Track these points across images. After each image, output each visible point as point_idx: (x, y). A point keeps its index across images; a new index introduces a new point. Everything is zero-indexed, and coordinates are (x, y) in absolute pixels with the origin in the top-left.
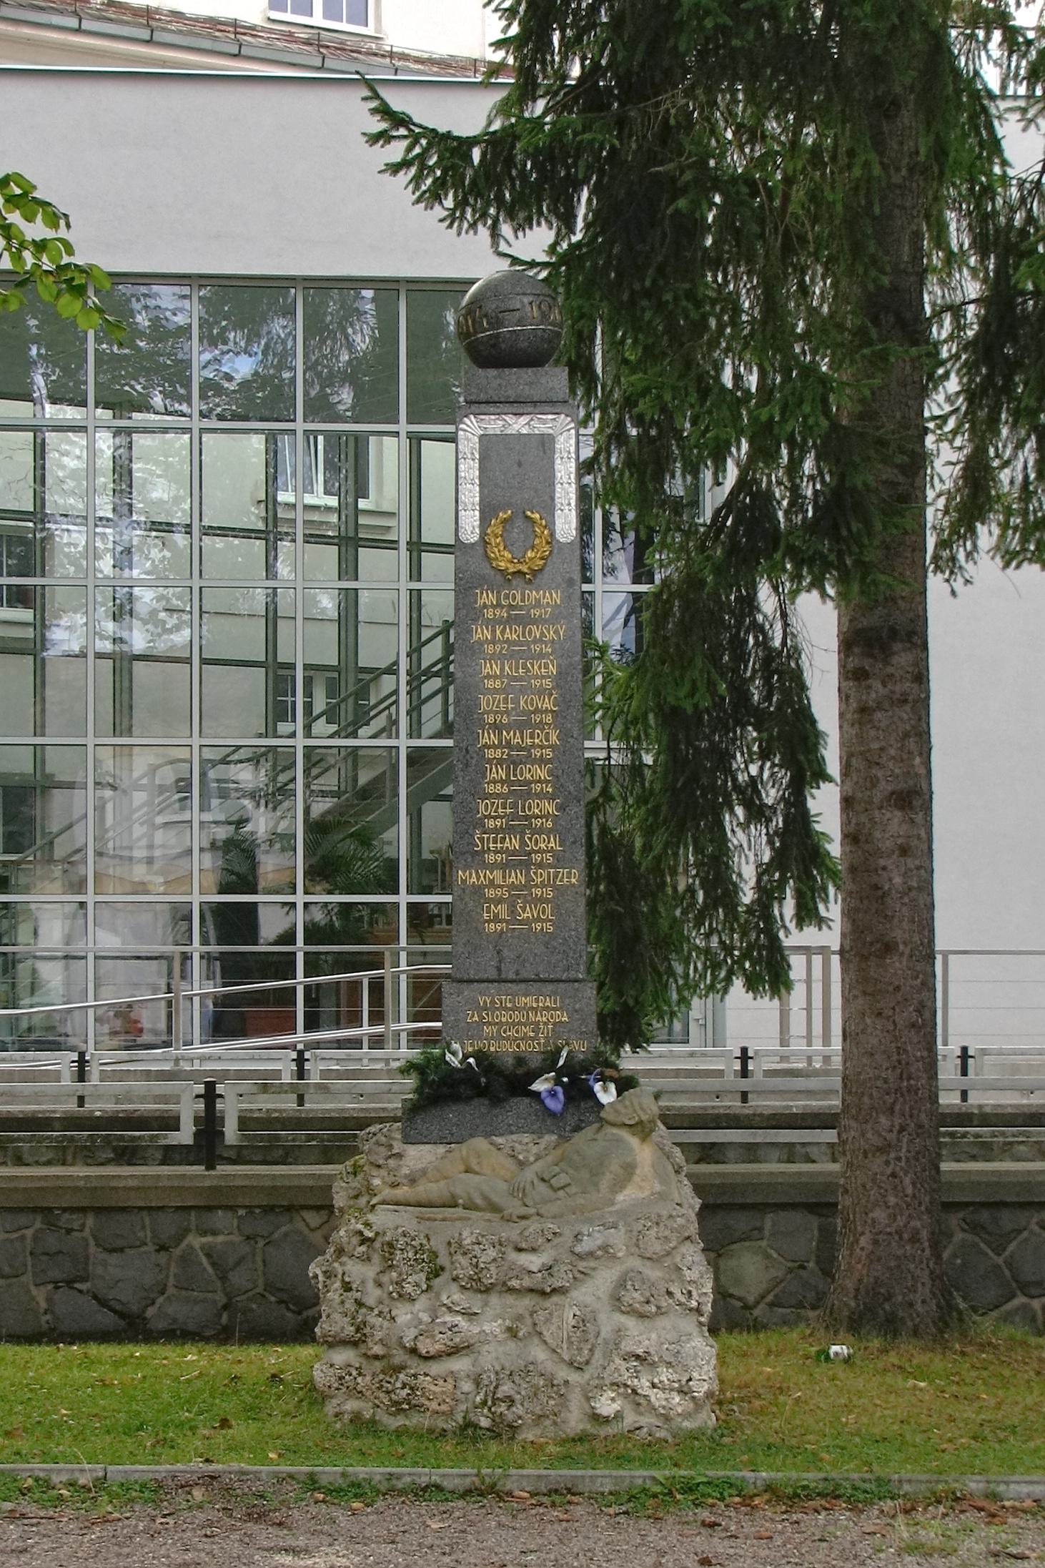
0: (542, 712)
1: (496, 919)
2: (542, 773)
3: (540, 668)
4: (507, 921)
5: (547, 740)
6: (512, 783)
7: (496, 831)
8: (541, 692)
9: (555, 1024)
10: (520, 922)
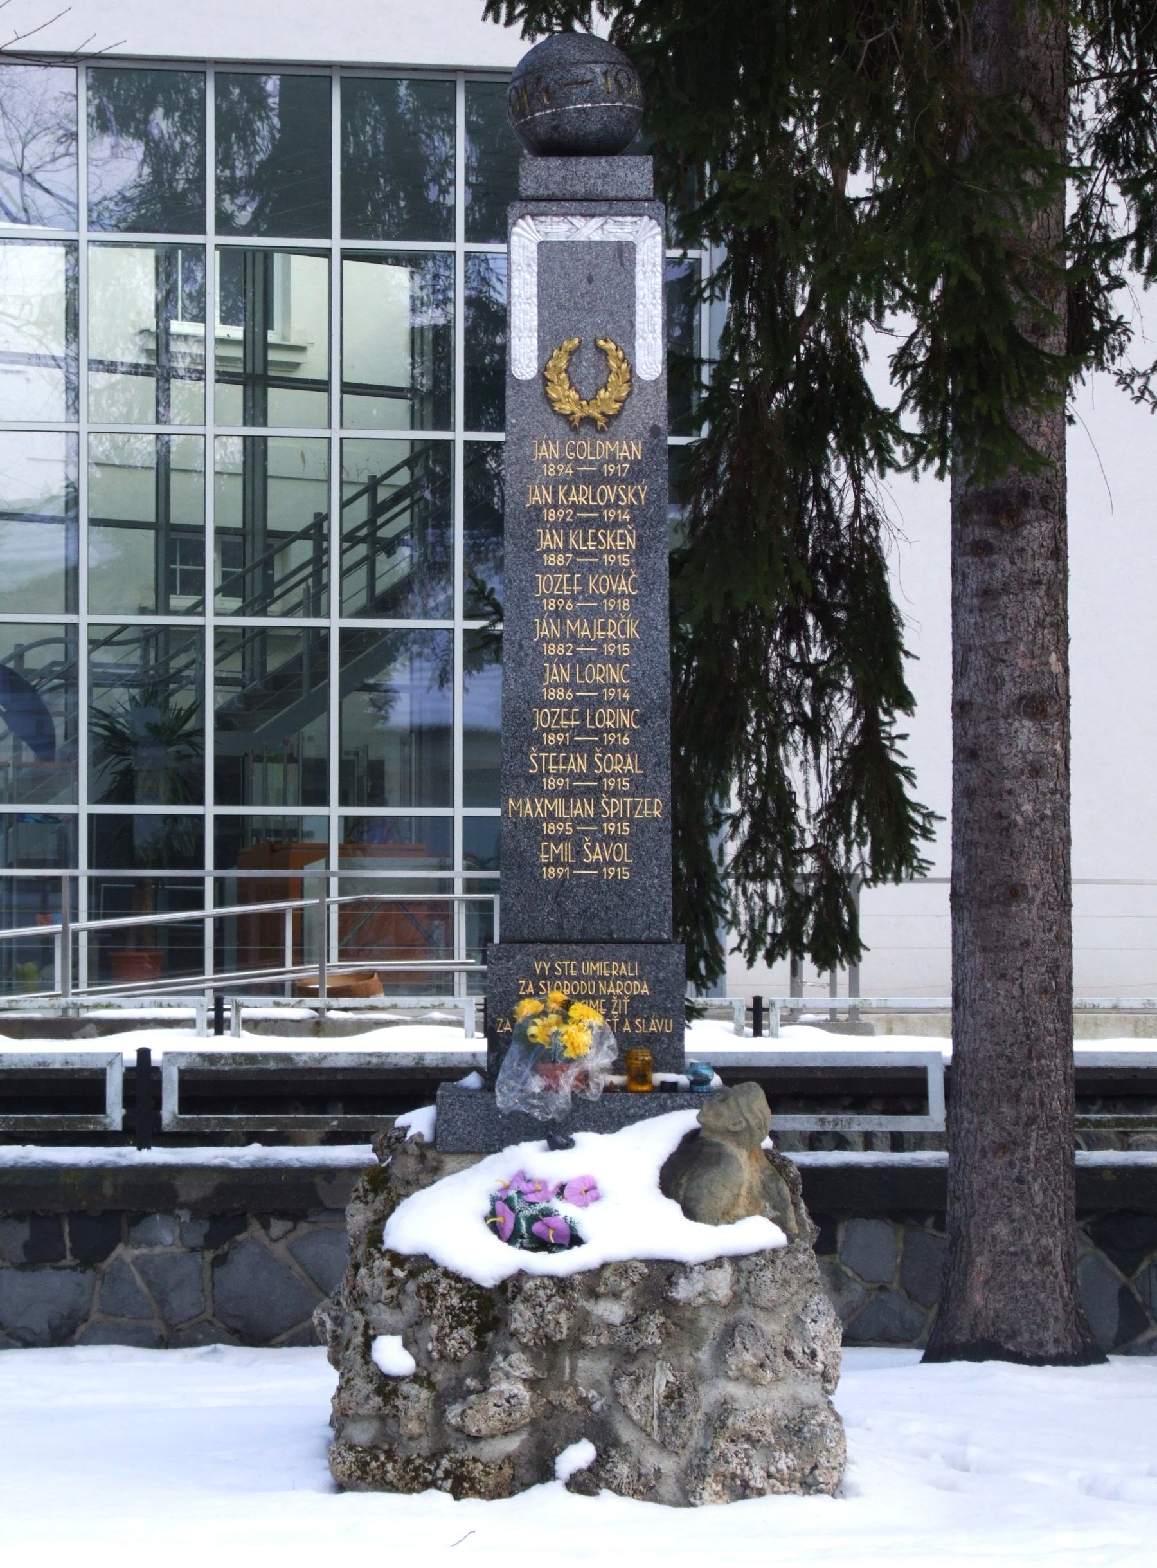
0: (617, 597)
1: (557, 862)
2: (616, 675)
3: (615, 540)
4: (571, 866)
5: (623, 632)
6: (580, 688)
7: (557, 748)
8: (615, 571)
9: (632, 998)
10: (588, 866)
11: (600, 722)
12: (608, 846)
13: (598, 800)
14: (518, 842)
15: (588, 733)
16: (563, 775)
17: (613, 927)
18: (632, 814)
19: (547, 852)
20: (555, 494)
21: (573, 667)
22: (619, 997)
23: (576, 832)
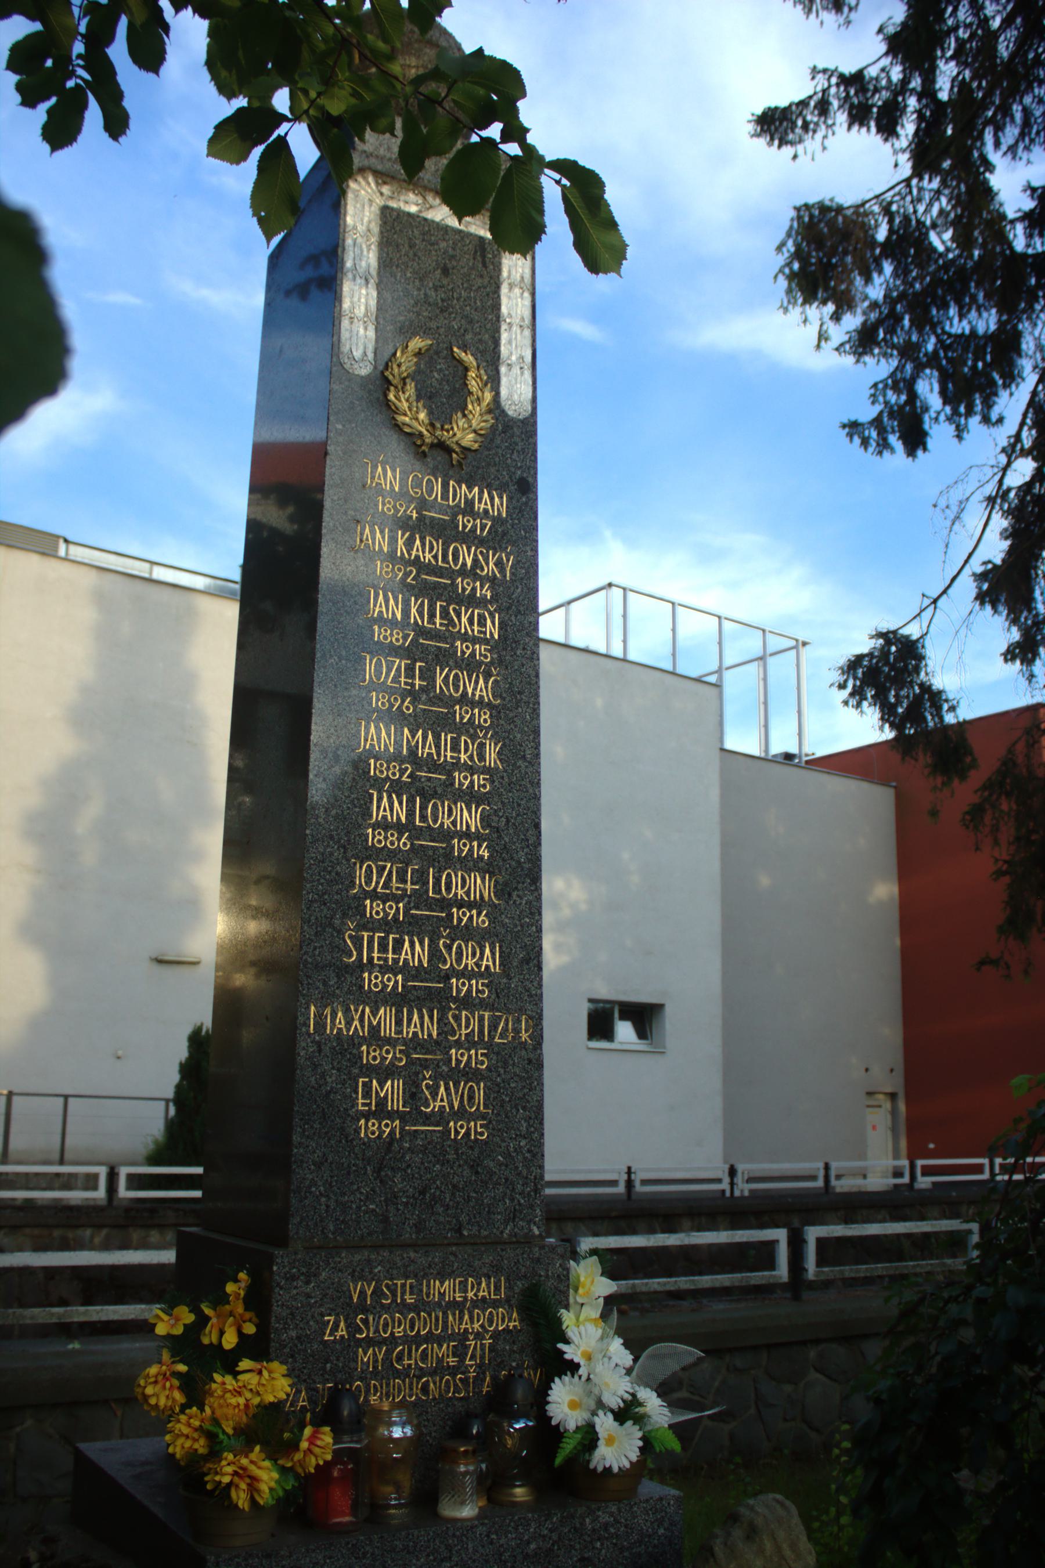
0: (473, 704)
1: (381, 1111)
2: (469, 818)
3: (471, 621)
4: (402, 1117)
5: (482, 758)
6: (416, 833)
7: (387, 925)
8: (471, 665)
9: (496, 1335)
10: (427, 1119)
11: (448, 888)
12: (456, 1085)
13: (443, 1011)
14: (323, 1075)
15: (429, 904)
16: (394, 970)
17: (463, 1218)
18: (491, 1037)
19: (367, 1094)
20: (393, 540)
21: (411, 801)
22: (478, 1336)
23: (411, 1062)
